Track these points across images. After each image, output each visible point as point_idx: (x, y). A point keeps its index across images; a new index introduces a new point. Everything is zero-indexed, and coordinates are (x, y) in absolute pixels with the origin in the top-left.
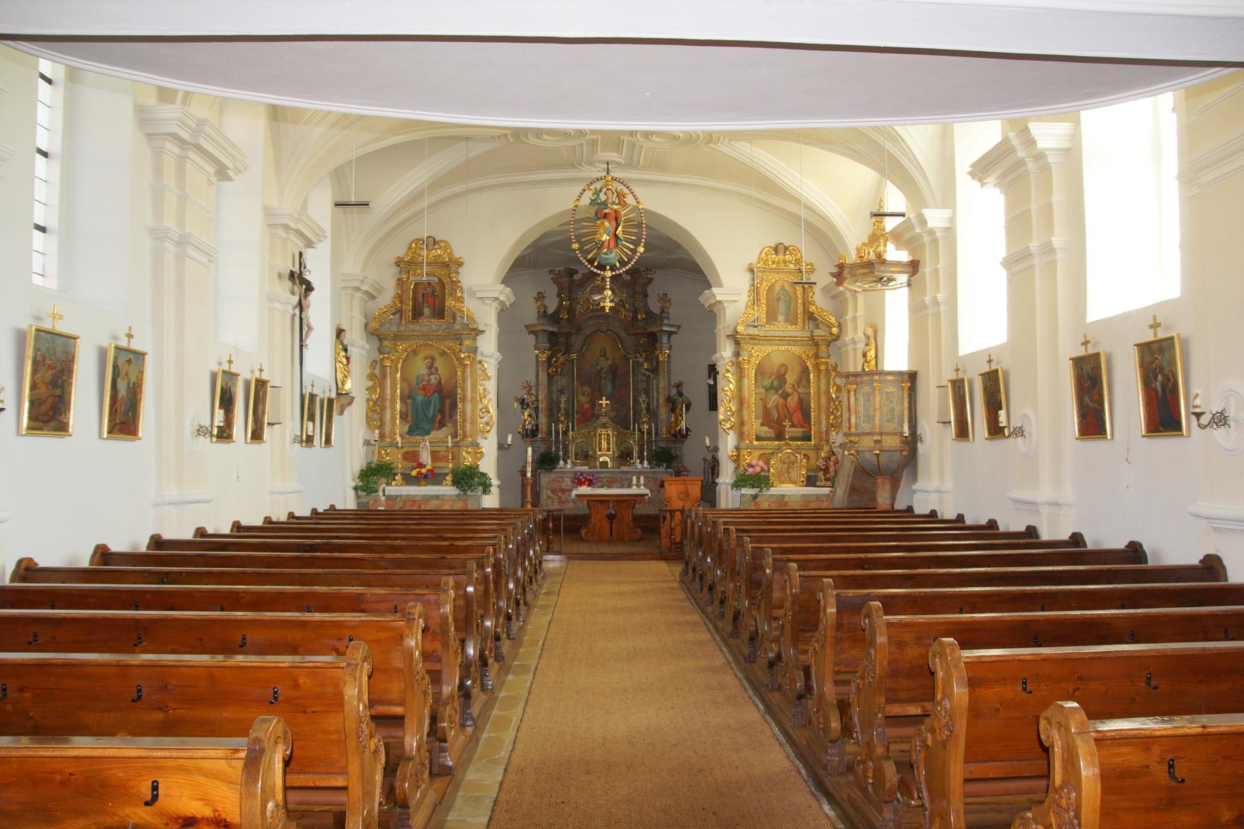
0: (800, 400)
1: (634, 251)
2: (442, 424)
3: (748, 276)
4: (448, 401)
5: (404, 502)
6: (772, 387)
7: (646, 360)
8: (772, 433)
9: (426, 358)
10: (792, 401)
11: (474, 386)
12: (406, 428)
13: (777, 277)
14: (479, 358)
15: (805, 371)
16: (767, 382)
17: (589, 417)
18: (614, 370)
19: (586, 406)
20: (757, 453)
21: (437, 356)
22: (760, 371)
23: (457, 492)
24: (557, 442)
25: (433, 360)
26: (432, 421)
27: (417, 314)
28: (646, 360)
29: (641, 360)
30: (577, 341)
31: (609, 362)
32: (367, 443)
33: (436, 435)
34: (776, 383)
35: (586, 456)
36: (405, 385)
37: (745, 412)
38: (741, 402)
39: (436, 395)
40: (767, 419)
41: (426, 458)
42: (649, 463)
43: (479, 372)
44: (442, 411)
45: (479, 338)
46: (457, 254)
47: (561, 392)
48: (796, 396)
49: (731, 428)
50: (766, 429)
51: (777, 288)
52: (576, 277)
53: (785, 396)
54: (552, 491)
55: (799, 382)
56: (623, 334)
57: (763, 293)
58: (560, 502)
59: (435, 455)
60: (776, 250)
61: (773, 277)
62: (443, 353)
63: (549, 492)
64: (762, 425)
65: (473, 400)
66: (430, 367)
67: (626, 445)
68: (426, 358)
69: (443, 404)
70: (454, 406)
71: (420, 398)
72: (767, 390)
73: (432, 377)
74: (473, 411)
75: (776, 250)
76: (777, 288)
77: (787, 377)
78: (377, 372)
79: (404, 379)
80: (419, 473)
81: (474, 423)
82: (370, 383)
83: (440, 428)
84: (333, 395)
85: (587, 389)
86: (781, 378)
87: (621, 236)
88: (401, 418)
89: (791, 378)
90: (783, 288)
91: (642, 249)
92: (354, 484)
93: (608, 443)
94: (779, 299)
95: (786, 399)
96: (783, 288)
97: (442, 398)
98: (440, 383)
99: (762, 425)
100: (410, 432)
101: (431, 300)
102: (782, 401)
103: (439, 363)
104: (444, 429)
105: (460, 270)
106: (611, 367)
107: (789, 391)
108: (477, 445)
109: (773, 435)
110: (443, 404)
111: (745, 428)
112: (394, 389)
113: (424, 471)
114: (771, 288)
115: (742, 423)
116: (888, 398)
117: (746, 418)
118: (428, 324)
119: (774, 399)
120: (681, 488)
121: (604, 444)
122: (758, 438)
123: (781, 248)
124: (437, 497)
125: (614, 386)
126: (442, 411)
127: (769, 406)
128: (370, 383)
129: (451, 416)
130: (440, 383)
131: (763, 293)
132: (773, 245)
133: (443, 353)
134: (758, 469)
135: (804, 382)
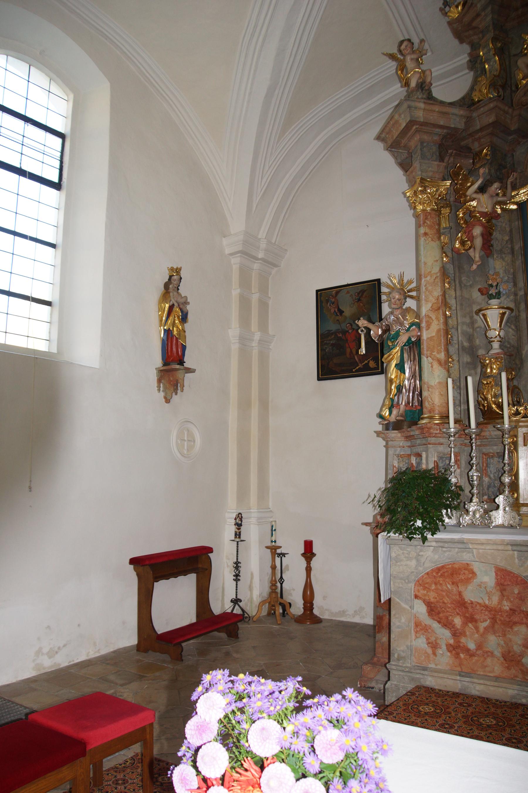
47: (488, 293)
54: (432, 610)
58: (456, 649)
63: (420, 608)
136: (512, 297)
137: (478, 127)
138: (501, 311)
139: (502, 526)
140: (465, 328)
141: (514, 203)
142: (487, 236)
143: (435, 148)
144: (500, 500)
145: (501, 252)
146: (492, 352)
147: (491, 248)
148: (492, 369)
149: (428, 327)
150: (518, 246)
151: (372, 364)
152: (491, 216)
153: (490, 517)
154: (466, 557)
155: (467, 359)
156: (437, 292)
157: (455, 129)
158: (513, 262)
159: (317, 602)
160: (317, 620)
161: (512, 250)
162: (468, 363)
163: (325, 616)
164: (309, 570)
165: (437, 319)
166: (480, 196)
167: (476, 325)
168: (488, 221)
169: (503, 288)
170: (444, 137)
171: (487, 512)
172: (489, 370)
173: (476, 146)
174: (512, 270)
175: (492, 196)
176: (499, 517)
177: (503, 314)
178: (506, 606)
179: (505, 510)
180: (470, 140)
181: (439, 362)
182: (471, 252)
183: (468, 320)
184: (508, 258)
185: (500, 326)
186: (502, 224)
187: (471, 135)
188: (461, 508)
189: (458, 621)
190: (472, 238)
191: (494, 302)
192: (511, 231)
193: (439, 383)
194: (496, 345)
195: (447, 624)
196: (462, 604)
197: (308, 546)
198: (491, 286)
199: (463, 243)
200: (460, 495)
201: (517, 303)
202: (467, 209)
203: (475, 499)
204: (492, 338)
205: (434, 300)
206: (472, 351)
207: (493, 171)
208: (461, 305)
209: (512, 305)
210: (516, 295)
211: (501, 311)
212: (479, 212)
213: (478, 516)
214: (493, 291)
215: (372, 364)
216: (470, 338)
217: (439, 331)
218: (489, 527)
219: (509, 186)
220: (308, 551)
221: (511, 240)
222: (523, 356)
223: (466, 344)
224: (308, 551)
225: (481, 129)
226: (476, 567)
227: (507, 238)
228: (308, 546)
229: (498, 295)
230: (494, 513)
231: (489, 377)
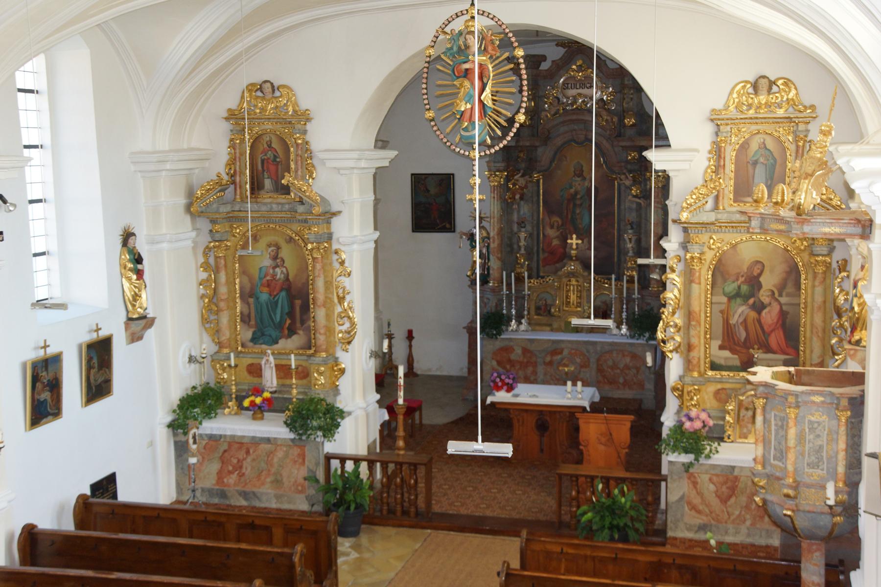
0: (783, 314)
1: (511, 121)
2: (292, 332)
3: (710, 128)
4: (298, 303)
5: (230, 445)
6: (738, 295)
7: (635, 182)
8: (735, 360)
9: (269, 246)
10: (770, 316)
11: (328, 284)
12: (249, 334)
13: (754, 128)
14: (335, 246)
15: (793, 274)
16: (731, 287)
19: (555, 242)
20: (712, 388)
21: (283, 244)
22: (719, 270)
23: (292, 436)
24: (509, 297)
25: (278, 248)
26: (280, 326)
27: (257, 187)
28: (635, 182)
29: (628, 183)
32: (191, 359)
33: (284, 344)
34: (745, 288)
36: (246, 279)
37: (693, 332)
38: (689, 316)
39: (283, 294)
40: (729, 341)
41: (270, 379)
42: (629, 328)
43: (336, 265)
44: (291, 314)
45: (335, 221)
46: (304, 105)
47: (521, 224)
48: (776, 308)
49: (676, 350)
50: (726, 353)
51: (754, 146)
52: (545, 66)
53: (759, 308)
54: (499, 363)
55: (782, 288)
57: (730, 154)
59: (283, 370)
60: (755, 86)
61: (747, 130)
62: (290, 240)
63: (494, 363)
64: (721, 348)
65: (328, 304)
66: (275, 258)
67: (604, 298)
68: (269, 246)
69: (292, 306)
70: (306, 308)
71: (264, 297)
72: (731, 298)
73: (278, 270)
74: (328, 317)
75: (755, 86)
76: (754, 146)
77: (761, 279)
78: (212, 261)
79: (244, 272)
80: (253, 403)
81: (330, 331)
82: (204, 275)
83: (289, 336)
84: (114, 327)
85: (556, 219)
86: (754, 282)
87: (489, 103)
88: (242, 320)
89: (769, 281)
90: (764, 146)
91: (521, 118)
92: (169, 419)
94: (755, 163)
95: (759, 313)
96: (764, 146)
97: (291, 298)
98: (287, 279)
99: (721, 348)
100: (254, 340)
101: (272, 168)
102: (753, 314)
103: (286, 253)
104: (295, 337)
105: (309, 126)
107: (766, 300)
108: (336, 360)
109: (737, 363)
110: (292, 306)
111: (694, 354)
112: (231, 285)
113: (258, 400)
114: (744, 147)
115: (690, 348)
116: (812, 430)
117: (694, 341)
118: (270, 200)
119: (741, 311)
120: (603, 427)
122: (714, 367)
123: (763, 83)
124: (268, 440)
126: (291, 314)
127: (733, 321)
128: (204, 275)
129: (303, 322)
130: (287, 279)
131: (730, 154)
132: (752, 79)
133: (290, 240)
134: (698, 425)
135: (790, 288)
149: (494, 242)
151: (448, 226)
154: (512, 344)
155: (509, 249)
159: (415, 365)
160: (416, 375)
163: (419, 373)
164: (410, 346)
176: (523, 327)
178: (525, 360)
188: (508, 324)
189: (508, 367)
191: (523, 230)
194: (523, 249)
195: (504, 368)
196: (509, 361)
197: (410, 332)
215: (448, 226)
220: (410, 336)
224: (410, 336)
226: (515, 348)
228: (410, 332)
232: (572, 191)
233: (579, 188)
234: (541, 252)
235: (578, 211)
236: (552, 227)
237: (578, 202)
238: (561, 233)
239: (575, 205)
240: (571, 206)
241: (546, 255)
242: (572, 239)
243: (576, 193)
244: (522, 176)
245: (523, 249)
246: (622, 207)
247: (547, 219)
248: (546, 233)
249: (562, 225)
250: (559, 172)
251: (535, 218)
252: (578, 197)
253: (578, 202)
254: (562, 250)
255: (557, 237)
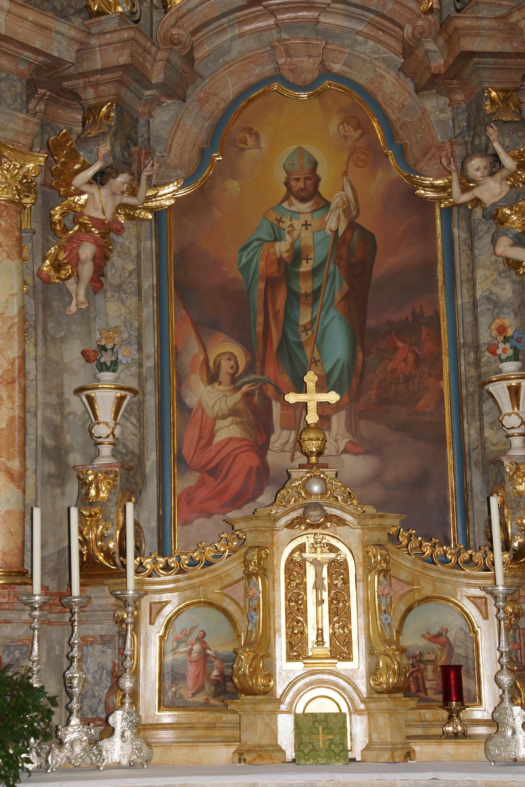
17: (242, 482)
18: (355, 252)
30: (176, 127)
31: (334, 222)
35: (226, 686)
47: (97, 358)
56: (393, 88)
85: (227, 350)
93: (339, 612)
106: (338, 242)
121: (317, 617)
125: (359, 335)
136: (134, 369)
137: (99, 66)
138: (119, 393)
139: (118, 766)
140: (49, 413)
141: (150, 210)
142: (101, 260)
143: (19, 87)
144: (118, 719)
145: (119, 288)
146: (100, 462)
147: (102, 279)
148: (98, 490)
150: (149, 282)
152: (109, 229)
153: (101, 751)
155: (50, 468)
156: (14, 352)
157: (60, 61)
158: (140, 309)
161: (139, 287)
162: (50, 476)
165: (11, 398)
166: (94, 189)
167: (67, 410)
168: (104, 235)
169: (125, 355)
170: (38, 69)
171: (94, 742)
172: (93, 492)
173: (89, 96)
174: (136, 324)
175: (114, 194)
176: (116, 750)
177: (121, 399)
179: (123, 736)
180: (81, 82)
181: (9, 473)
182: (71, 284)
183: (54, 400)
184: (132, 301)
185: (115, 418)
186: (126, 241)
187: (84, 75)
190: (75, 261)
191: (107, 376)
192: (138, 255)
193: (9, 512)
194: (106, 450)
198: (104, 348)
199: (57, 266)
200: (53, 713)
201: (141, 379)
202: (70, 208)
203: (75, 721)
204: (100, 437)
205: (6, 365)
206: (57, 454)
207: (118, 149)
208: (45, 372)
209: (133, 383)
210: (140, 365)
211: (119, 393)
212: (91, 218)
213: (78, 749)
214: (107, 358)
216: (56, 431)
217: (12, 420)
218: (98, 767)
219: (143, 181)
221: (138, 271)
222: (147, 470)
223: (49, 442)
225: (104, 71)
227: (131, 267)
229: (113, 367)
230: (105, 744)
231: (92, 504)
232: (282, 248)
233: (306, 238)
234: (172, 468)
235: (305, 317)
236: (213, 378)
237: (305, 287)
238: (248, 395)
239: (293, 297)
240: (281, 302)
241: (191, 479)
242: (301, 388)
243: (298, 255)
244: (100, 179)
245: (106, 450)
246: (463, 300)
247: (195, 347)
248: (191, 401)
249: (250, 368)
250: (233, 186)
251: (150, 347)
252: (305, 267)
253: (305, 287)
254: (249, 460)
255: (233, 412)
